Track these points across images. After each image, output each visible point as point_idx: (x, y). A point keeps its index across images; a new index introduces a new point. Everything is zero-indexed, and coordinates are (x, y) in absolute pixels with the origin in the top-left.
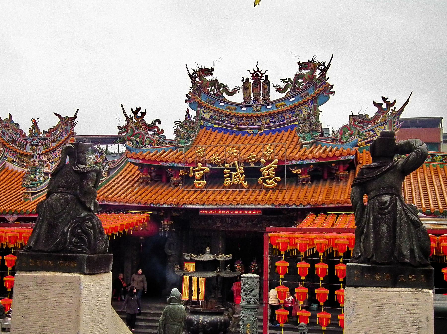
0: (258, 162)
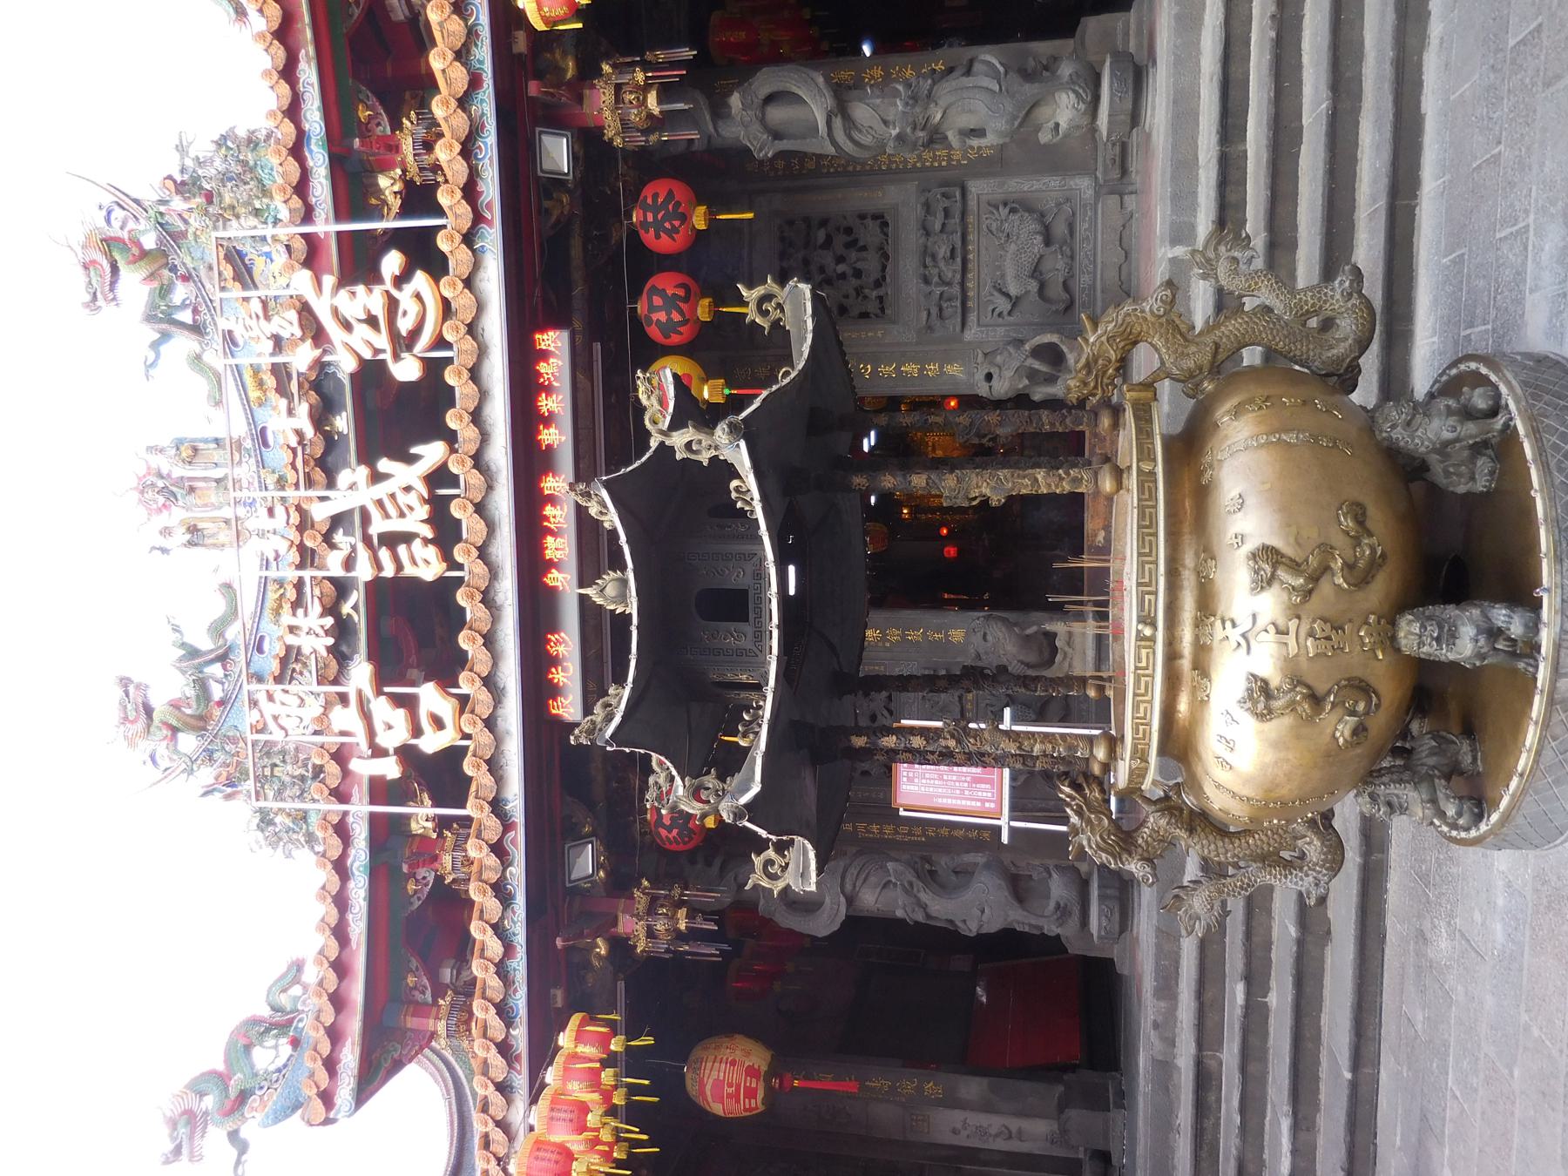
0: (320, 383)
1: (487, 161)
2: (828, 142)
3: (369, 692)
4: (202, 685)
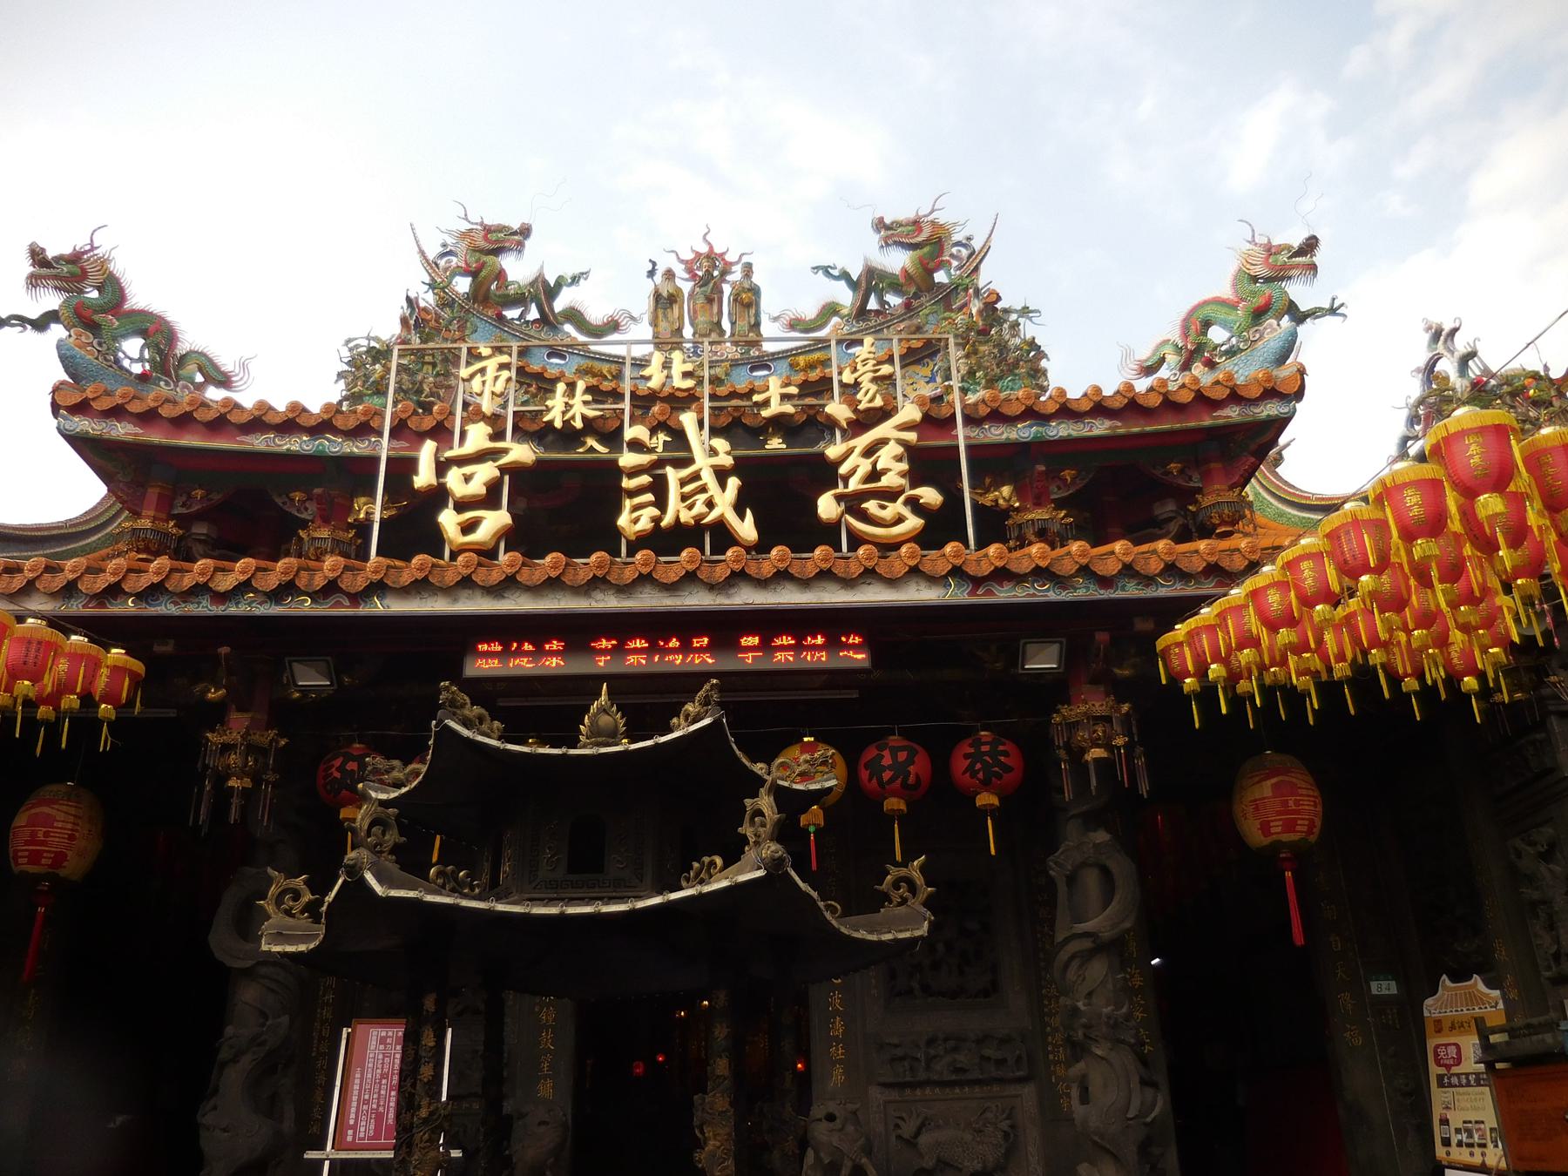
0: (814, 425)
1: (1032, 591)
2: (1068, 934)
3: (504, 460)
4: (520, 300)
